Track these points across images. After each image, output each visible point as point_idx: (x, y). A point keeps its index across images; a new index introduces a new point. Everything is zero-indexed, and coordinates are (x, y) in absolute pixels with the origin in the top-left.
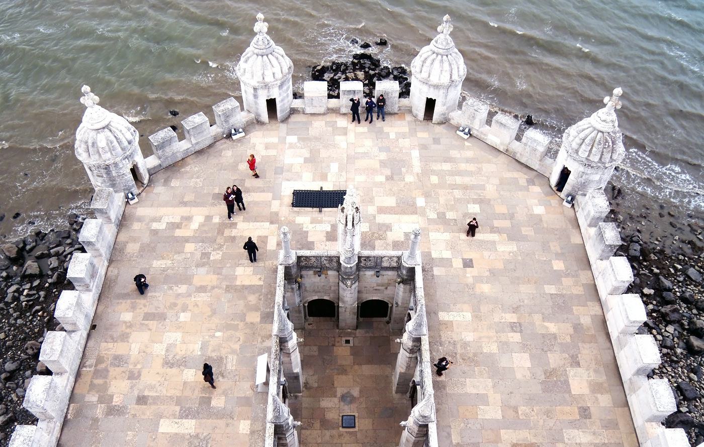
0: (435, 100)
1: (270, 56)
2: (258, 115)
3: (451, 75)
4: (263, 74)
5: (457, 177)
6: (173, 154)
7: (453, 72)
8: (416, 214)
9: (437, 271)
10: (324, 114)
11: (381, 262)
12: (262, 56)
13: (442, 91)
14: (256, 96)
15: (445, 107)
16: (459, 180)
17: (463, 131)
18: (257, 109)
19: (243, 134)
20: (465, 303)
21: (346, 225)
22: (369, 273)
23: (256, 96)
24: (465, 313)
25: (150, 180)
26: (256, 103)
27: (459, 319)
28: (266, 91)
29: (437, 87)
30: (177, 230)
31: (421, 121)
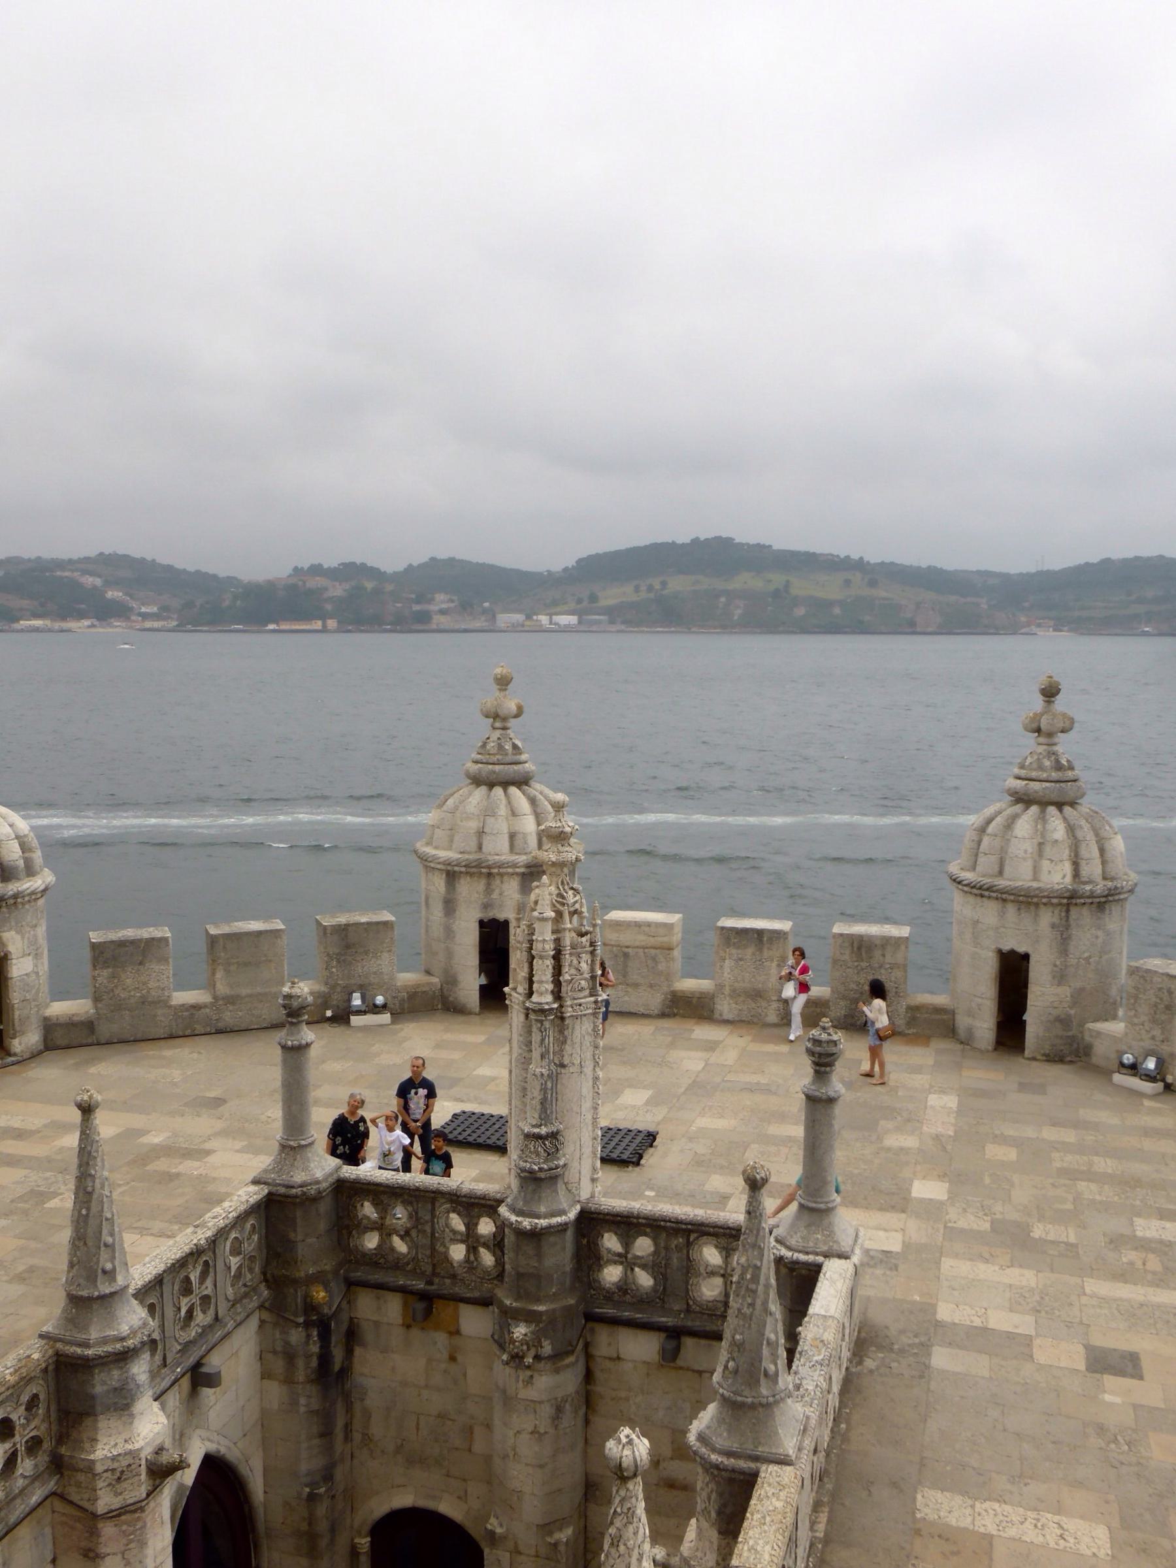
0: (1026, 957)
1: (513, 790)
2: (451, 980)
3: (1076, 865)
4: (481, 833)
5: (1096, 1159)
6: (144, 1001)
7: (1084, 852)
8: (903, 1212)
9: (941, 1358)
10: (663, 1015)
11: (690, 1268)
12: (491, 785)
13: (1047, 918)
14: (450, 905)
15: (1065, 992)
16: (1104, 1165)
17: (1133, 1069)
18: (450, 954)
19: (386, 1018)
20: (1078, 1484)
21: (530, 993)
22: (639, 1348)
23: (450, 905)
24: (1071, 1524)
25: (35, 1056)
26: (449, 933)
27: (1031, 1535)
28: (481, 885)
29: (1027, 900)
30: (10, 1142)
31: (981, 1051)
